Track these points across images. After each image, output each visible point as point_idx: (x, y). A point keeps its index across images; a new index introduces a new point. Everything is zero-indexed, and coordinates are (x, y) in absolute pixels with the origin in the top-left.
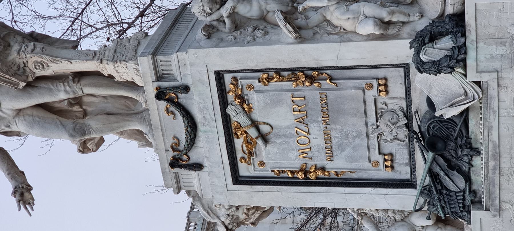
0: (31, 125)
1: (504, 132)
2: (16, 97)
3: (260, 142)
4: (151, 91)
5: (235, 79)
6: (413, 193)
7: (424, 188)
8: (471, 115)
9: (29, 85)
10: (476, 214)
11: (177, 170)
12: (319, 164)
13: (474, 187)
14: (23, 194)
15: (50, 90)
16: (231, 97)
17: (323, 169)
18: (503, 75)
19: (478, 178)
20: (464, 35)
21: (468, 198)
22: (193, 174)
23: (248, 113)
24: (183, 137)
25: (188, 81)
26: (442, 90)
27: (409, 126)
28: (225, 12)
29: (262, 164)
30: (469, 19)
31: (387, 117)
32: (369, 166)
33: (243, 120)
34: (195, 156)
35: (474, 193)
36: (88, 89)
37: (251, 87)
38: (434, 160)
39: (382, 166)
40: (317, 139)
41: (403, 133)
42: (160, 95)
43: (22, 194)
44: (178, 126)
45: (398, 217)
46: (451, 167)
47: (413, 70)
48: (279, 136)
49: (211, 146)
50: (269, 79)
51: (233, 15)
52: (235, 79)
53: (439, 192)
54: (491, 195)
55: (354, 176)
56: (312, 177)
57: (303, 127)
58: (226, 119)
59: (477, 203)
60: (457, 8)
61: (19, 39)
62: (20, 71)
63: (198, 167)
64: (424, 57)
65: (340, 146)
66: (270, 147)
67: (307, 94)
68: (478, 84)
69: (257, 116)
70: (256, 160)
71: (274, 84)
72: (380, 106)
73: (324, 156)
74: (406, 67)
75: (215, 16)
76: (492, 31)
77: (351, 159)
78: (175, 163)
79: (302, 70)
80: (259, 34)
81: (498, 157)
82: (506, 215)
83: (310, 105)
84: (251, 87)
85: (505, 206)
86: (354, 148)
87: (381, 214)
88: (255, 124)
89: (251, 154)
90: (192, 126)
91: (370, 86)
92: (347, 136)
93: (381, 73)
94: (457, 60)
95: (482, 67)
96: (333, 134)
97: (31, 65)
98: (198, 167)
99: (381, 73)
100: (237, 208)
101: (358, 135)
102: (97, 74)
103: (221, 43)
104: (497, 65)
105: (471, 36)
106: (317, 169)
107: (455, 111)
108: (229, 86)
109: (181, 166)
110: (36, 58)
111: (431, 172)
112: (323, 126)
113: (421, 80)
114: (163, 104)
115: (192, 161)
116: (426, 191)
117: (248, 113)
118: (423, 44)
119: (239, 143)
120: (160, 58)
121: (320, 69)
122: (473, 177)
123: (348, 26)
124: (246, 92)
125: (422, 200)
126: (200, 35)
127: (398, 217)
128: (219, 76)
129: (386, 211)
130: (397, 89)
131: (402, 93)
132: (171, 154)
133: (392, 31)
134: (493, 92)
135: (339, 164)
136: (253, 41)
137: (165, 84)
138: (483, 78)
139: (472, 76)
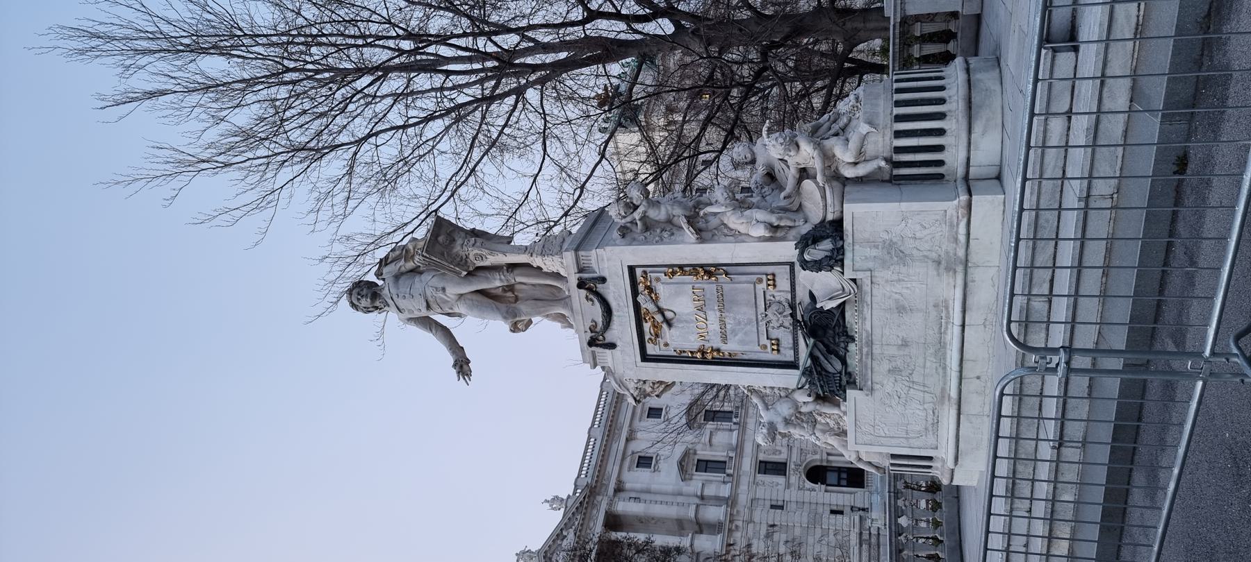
0: (472, 307)
1: (876, 323)
2: (459, 284)
3: (665, 326)
4: (573, 280)
5: (645, 272)
6: (797, 373)
7: (806, 369)
8: (847, 307)
9: (470, 274)
10: (850, 393)
11: (594, 348)
12: (715, 346)
13: (850, 370)
14: (462, 366)
15: (487, 278)
16: (641, 287)
17: (718, 350)
18: (876, 274)
19: (853, 361)
20: (842, 238)
21: (844, 379)
22: (608, 351)
23: (655, 301)
24: (600, 320)
25: (605, 274)
26: (822, 285)
27: (793, 315)
28: (637, 215)
29: (666, 345)
30: (847, 225)
31: (774, 307)
32: (758, 349)
33: (651, 307)
34: (610, 337)
35: (849, 374)
36: (519, 278)
37: (658, 279)
38: (815, 345)
39: (769, 349)
40: (714, 326)
41: (788, 321)
42: (581, 284)
43: (461, 367)
44: (597, 311)
45: (783, 394)
46: (830, 351)
47: (797, 267)
48: (681, 322)
49: (623, 329)
50: (674, 273)
51: (644, 218)
52: (645, 272)
53: (819, 373)
54: (864, 376)
55: (745, 357)
56: (709, 357)
57: (701, 314)
58: (637, 306)
59: (852, 383)
60: (837, 215)
61: (463, 234)
62: (463, 262)
64: (807, 257)
65: (733, 331)
66: (673, 330)
67: (705, 286)
68: (854, 280)
69: (662, 304)
70: (662, 342)
71: (677, 278)
72: (768, 297)
73: (719, 339)
74: (792, 265)
75: (629, 219)
76: (866, 235)
77: (742, 342)
78: (592, 343)
79: (702, 266)
80: (665, 234)
81: (870, 344)
82: (877, 394)
83: (708, 296)
84: (658, 279)
85: (876, 387)
86: (746, 333)
87: (768, 391)
88: (661, 311)
89: (657, 336)
90: (608, 311)
91: (760, 281)
92: (739, 323)
93: (770, 269)
94: (835, 260)
95: (857, 266)
97: (471, 257)
98: (612, 346)
99: (770, 269)
100: (645, 382)
101: (750, 322)
102: (528, 266)
103: (633, 241)
104: (870, 265)
105: (848, 240)
106: (713, 350)
107: (834, 304)
108: (640, 278)
109: (597, 346)
110: (476, 251)
111: (811, 355)
112: (718, 314)
113: (803, 276)
114: (583, 292)
115: (607, 341)
116: (807, 372)
117: (655, 301)
118: (807, 246)
119: (647, 326)
120: (581, 253)
121: (717, 266)
122: (849, 361)
123: (742, 229)
124: (654, 283)
125: (804, 380)
126: (616, 234)
127: (783, 394)
128: (632, 269)
129: (772, 388)
130: (783, 284)
131: (788, 288)
132: (589, 334)
133: (779, 234)
134: (867, 288)
135: (732, 347)
136: (661, 241)
137: (585, 275)
138: (858, 276)
139: (849, 274)
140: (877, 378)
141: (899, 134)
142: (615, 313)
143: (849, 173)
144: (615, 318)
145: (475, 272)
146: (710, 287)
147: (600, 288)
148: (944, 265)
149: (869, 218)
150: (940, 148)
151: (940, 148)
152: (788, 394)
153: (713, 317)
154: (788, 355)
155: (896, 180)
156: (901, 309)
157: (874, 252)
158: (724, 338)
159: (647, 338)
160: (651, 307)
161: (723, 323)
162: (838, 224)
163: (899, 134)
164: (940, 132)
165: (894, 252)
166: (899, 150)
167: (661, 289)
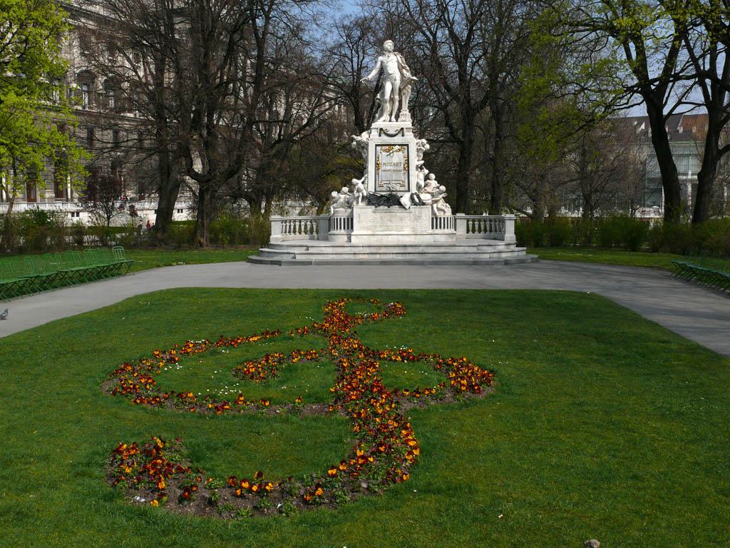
19: (381, 207)
23: (396, 151)
33: (394, 150)
34: (383, 135)
40: (388, 168)
42: (402, 129)
59: (376, 207)
63: (380, 136)
74: (409, 191)
78: (381, 129)
96: (390, 172)
98: (380, 136)
99: (407, 185)
111: (382, 196)
114: (399, 129)
117: (396, 151)
119: (387, 147)
128: (408, 145)
130: (402, 189)
137: (405, 130)
140: (379, 214)
141: (444, 218)
142: (392, 138)
143: (435, 206)
144: (390, 138)
145: (400, 90)
146: (402, 168)
147: (400, 135)
148: (414, 229)
149: (426, 213)
150: (440, 228)
151: (440, 228)
152: (366, 189)
153: (392, 168)
154: (378, 189)
155: (433, 219)
156: (401, 220)
157: (417, 214)
158: (385, 171)
159: (384, 147)
160: (394, 150)
161: (389, 170)
162: (424, 204)
163: (444, 218)
164: (444, 228)
165: (418, 218)
166: (440, 218)
167: (401, 153)
